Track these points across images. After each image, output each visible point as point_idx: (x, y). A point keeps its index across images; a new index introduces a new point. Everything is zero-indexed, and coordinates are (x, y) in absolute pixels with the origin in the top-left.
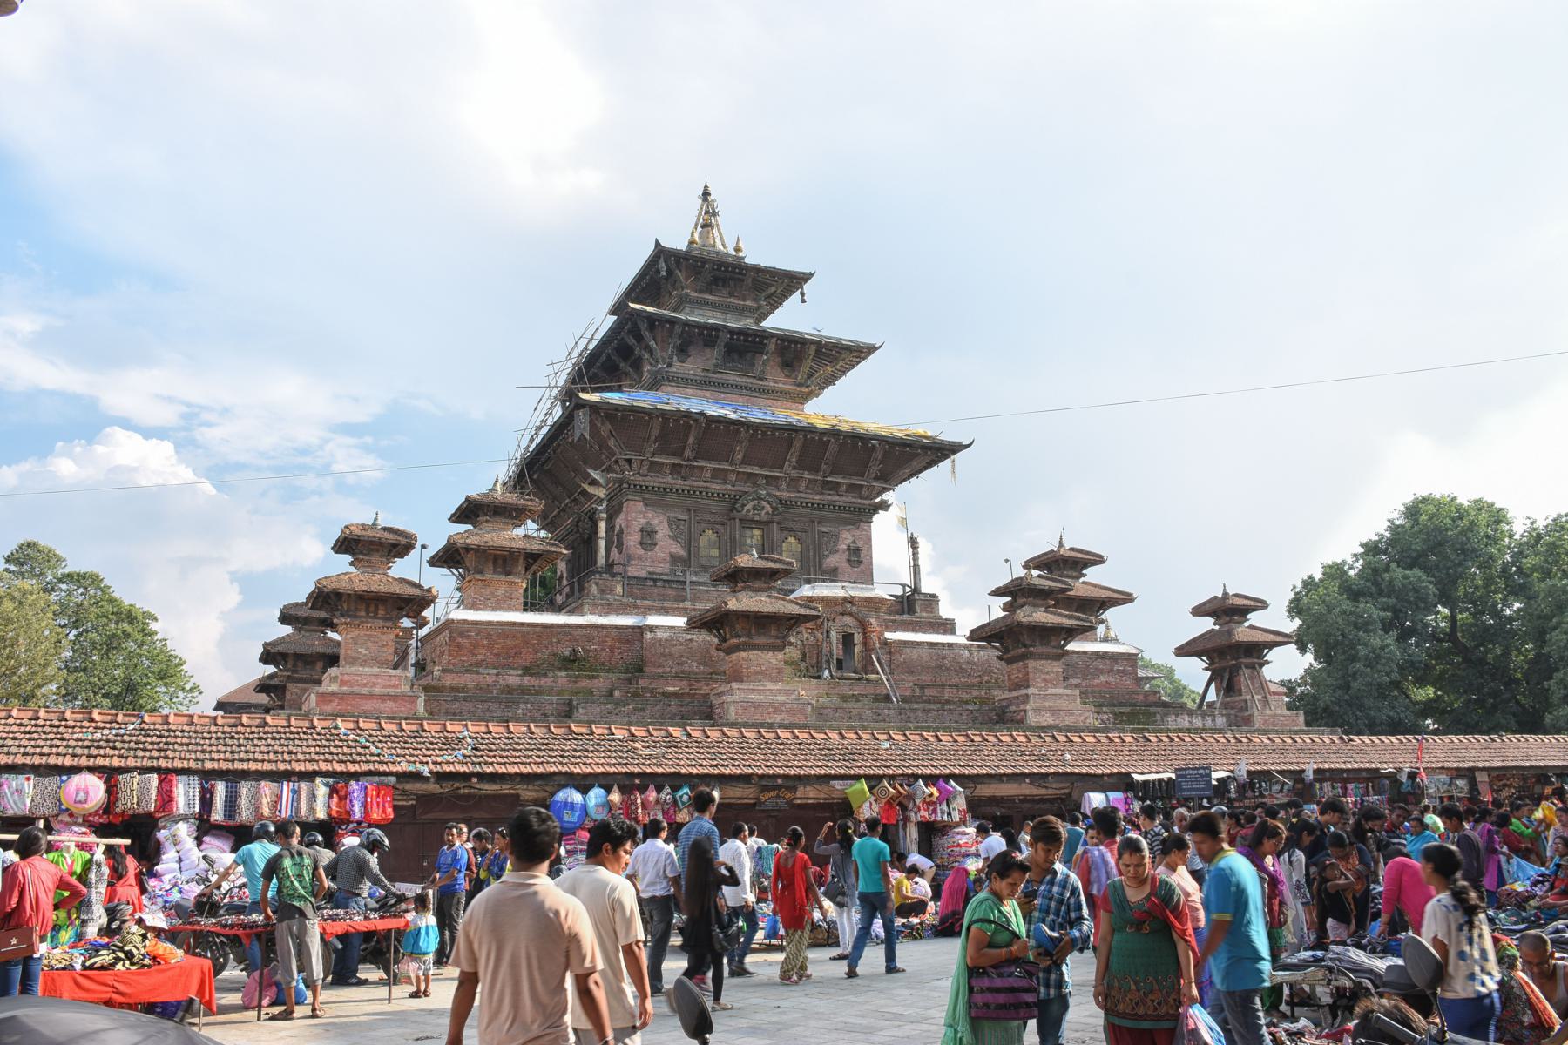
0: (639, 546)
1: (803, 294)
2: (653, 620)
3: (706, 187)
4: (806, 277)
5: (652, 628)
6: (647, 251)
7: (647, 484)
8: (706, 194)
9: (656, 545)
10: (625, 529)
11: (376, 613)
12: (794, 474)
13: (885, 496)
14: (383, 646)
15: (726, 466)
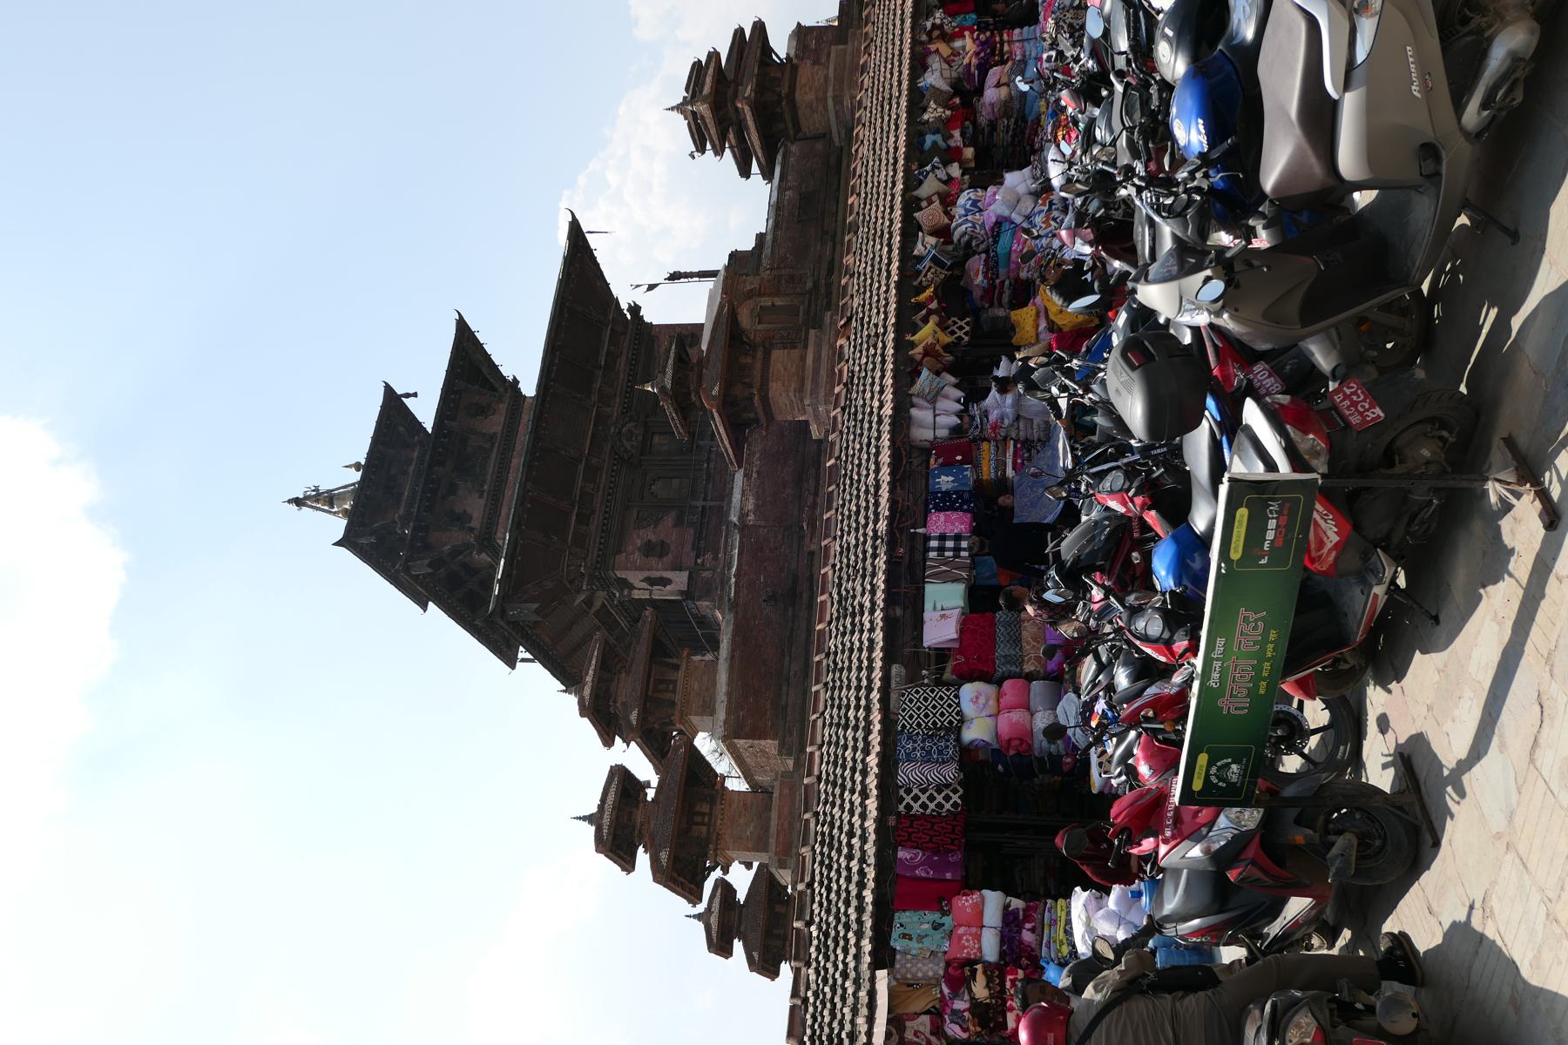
0: (665, 559)
1: (408, 395)
2: (734, 518)
3: (290, 501)
4: (389, 390)
5: (743, 516)
6: (346, 556)
7: (596, 550)
8: (298, 502)
9: (662, 541)
10: (646, 574)
11: (703, 814)
12: (594, 398)
13: (624, 306)
14: (745, 805)
15: (581, 467)
